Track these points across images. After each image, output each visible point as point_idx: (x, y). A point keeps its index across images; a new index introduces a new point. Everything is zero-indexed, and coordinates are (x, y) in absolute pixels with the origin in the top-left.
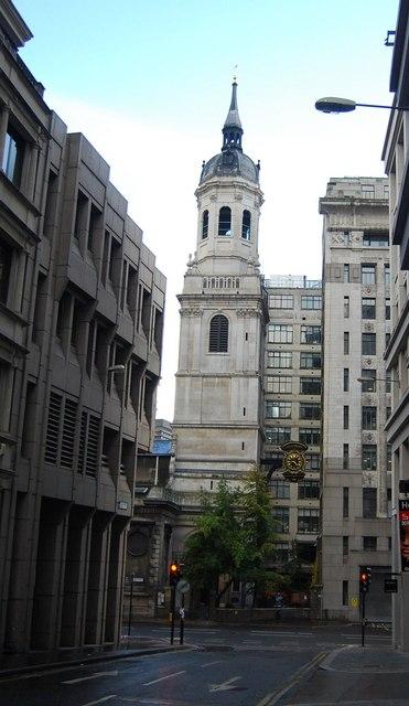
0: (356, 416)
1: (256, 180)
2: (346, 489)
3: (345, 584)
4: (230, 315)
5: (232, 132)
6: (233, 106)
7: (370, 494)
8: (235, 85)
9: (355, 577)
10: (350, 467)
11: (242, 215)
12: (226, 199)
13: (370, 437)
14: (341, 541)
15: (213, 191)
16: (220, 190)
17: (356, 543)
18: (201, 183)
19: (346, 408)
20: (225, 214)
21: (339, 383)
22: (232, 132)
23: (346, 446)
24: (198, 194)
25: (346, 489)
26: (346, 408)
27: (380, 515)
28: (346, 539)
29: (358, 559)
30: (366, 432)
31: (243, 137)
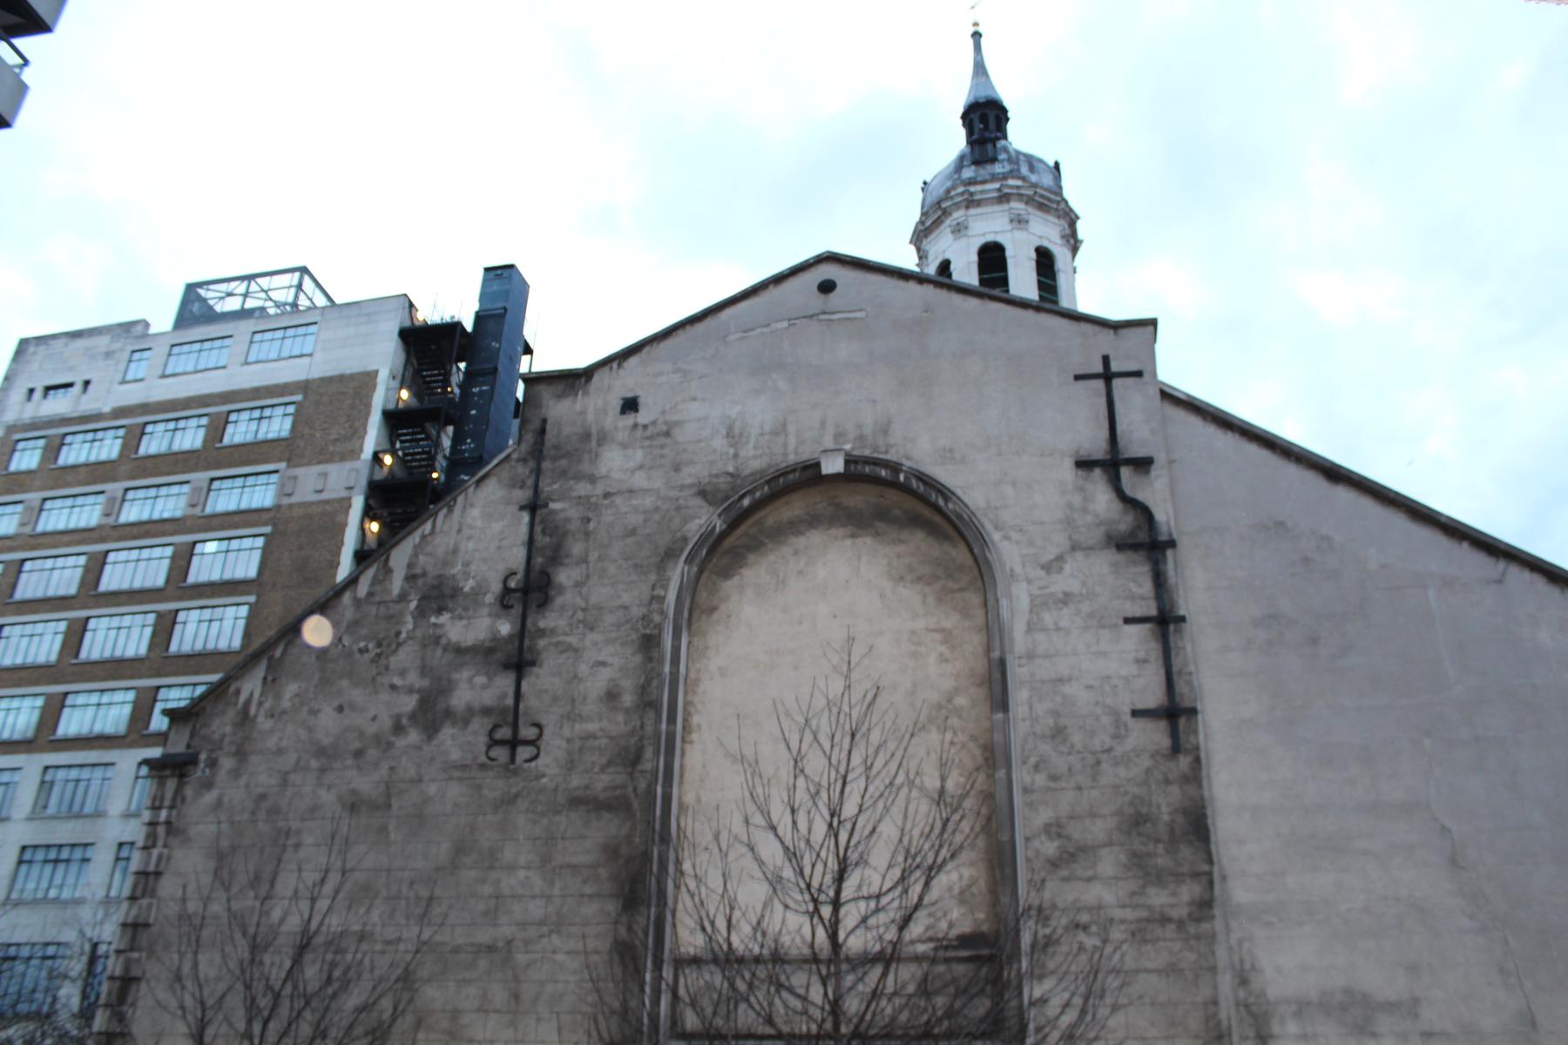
1: (1058, 190)
5: (985, 119)
6: (980, 69)
8: (977, 36)
11: (1034, 255)
12: (989, 225)
15: (958, 215)
16: (972, 211)
18: (924, 214)
20: (992, 259)
22: (985, 119)
24: (921, 236)
31: (1010, 127)
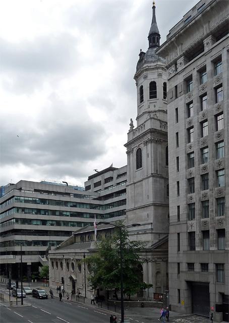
0: (184, 185)
2: (179, 234)
3: (179, 290)
4: (142, 146)
7: (191, 235)
9: (183, 286)
10: (180, 220)
13: (191, 198)
14: (176, 266)
17: (184, 267)
19: (178, 183)
21: (174, 168)
23: (179, 207)
25: (179, 234)
26: (178, 183)
27: (197, 249)
28: (179, 264)
29: (185, 277)
30: (189, 195)
